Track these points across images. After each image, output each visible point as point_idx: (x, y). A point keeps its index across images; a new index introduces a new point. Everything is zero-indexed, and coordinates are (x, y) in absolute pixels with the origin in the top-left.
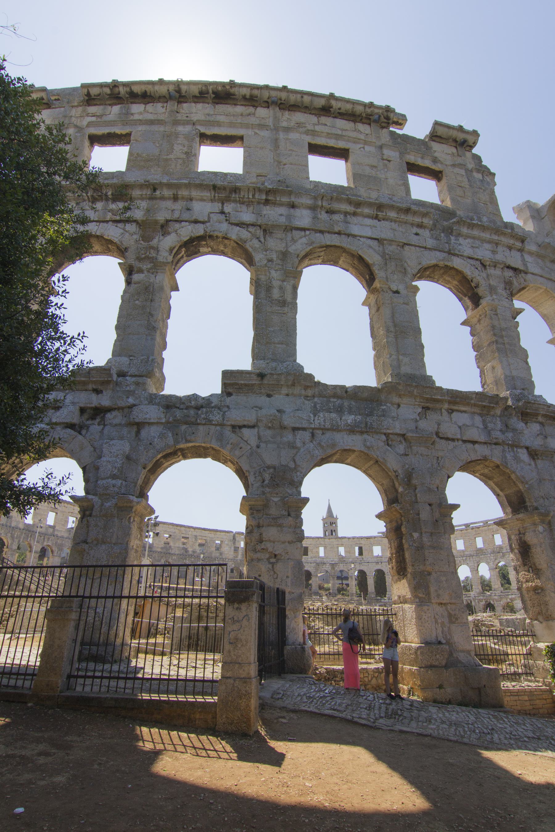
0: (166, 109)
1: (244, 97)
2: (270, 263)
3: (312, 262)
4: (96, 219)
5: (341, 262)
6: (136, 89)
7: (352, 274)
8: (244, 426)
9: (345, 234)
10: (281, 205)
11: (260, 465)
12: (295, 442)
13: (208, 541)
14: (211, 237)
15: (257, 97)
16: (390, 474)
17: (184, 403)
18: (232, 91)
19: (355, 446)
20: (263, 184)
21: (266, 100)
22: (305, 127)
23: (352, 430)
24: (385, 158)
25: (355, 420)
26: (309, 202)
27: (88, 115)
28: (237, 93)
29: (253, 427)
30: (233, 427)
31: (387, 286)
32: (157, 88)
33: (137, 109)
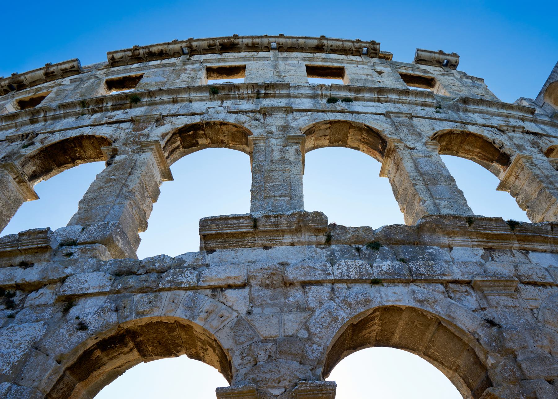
6: (154, 49)
7: (363, 151)
11: (253, 339)
12: (306, 302)
15: (258, 44)
16: (465, 339)
18: (236, 41)
19: (400, 301)
28: (240, 43)
31: (403, 145)
32: (171, 46)
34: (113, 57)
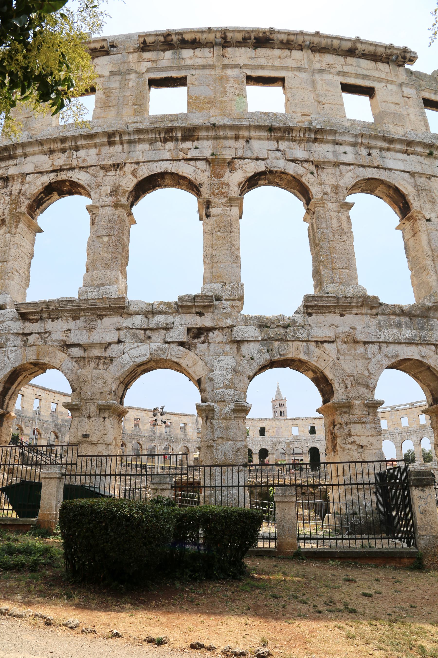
0: (213, 54)
1: (282, 42)
2: (325, 196)
3: (354, 191)
4: (171, 158)
5: (376, 192)
7: (385, 201)
8: (325, 342)
9: (383, 168)
10: (327, 142)
13: (173, 424)
14: (271, 172)
15: (293, 41)
17: (273, 323)
18: (271, 37)
20: (310, 123)
21: (300, 44)
22: (335, 67)
23: (410, 343)
24: (405, 95)
25: (412, 334)
26: (352, 139)
27: (144, 60)
28: (275, 39)
29: (332, 342)
30: (317, 342)
32: (205, 35)
33: (187, 53)
34: (145, 41)
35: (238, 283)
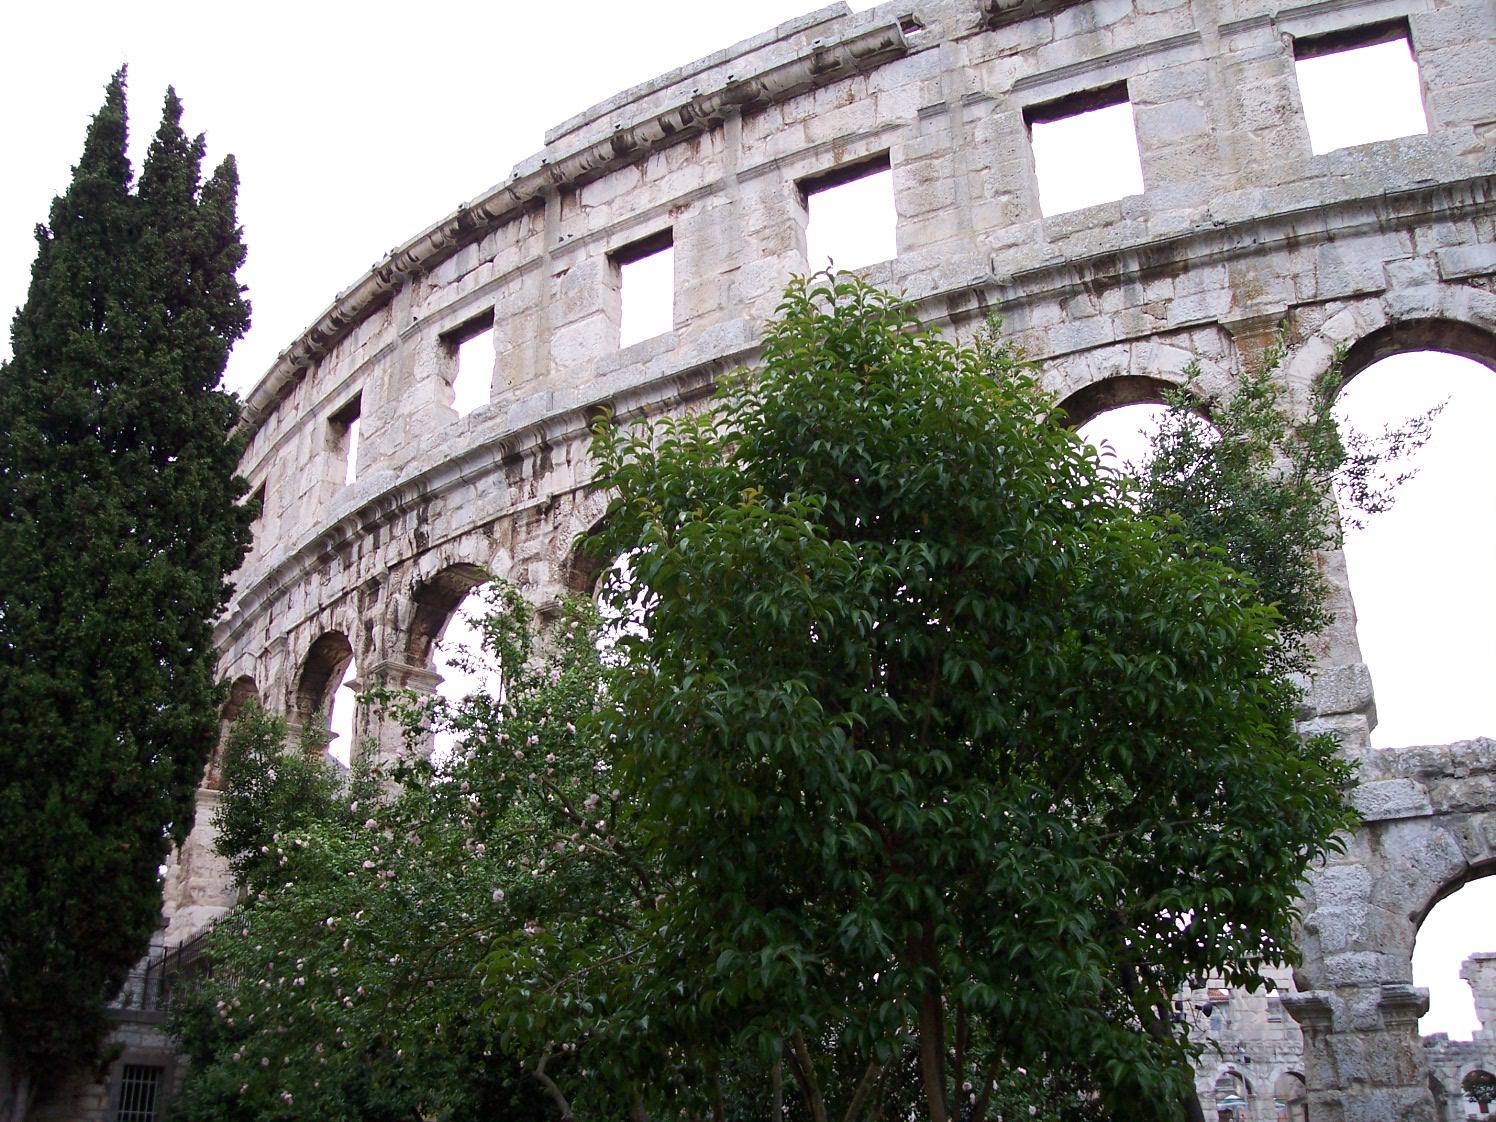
4: (1123, 337)
17: (1462, 764)
27: (1001, 54)
35: (1351, 667)
